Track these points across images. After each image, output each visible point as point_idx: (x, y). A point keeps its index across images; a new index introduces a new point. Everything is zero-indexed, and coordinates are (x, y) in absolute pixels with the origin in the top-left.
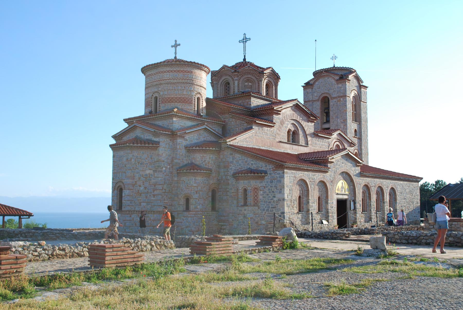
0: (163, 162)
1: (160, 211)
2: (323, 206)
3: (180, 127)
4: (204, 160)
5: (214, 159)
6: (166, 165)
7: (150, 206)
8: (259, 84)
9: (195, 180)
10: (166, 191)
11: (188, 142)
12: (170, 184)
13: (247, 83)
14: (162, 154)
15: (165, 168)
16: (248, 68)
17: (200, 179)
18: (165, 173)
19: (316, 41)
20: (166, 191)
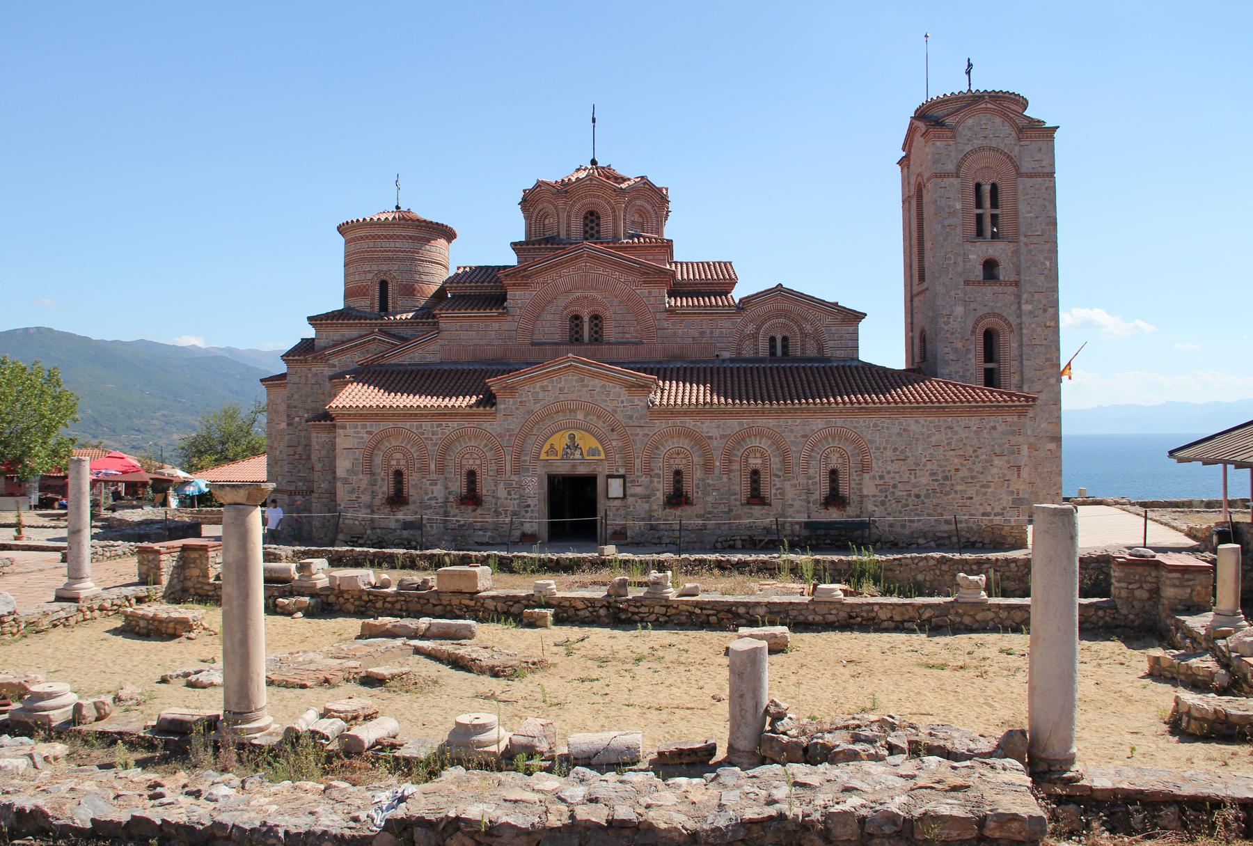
1: (291, 492)
2: (484, 492)
6: (300, 414)
10: (303, 457)
11: (337, 369)
18: (299, 427)
19: (926, 36)
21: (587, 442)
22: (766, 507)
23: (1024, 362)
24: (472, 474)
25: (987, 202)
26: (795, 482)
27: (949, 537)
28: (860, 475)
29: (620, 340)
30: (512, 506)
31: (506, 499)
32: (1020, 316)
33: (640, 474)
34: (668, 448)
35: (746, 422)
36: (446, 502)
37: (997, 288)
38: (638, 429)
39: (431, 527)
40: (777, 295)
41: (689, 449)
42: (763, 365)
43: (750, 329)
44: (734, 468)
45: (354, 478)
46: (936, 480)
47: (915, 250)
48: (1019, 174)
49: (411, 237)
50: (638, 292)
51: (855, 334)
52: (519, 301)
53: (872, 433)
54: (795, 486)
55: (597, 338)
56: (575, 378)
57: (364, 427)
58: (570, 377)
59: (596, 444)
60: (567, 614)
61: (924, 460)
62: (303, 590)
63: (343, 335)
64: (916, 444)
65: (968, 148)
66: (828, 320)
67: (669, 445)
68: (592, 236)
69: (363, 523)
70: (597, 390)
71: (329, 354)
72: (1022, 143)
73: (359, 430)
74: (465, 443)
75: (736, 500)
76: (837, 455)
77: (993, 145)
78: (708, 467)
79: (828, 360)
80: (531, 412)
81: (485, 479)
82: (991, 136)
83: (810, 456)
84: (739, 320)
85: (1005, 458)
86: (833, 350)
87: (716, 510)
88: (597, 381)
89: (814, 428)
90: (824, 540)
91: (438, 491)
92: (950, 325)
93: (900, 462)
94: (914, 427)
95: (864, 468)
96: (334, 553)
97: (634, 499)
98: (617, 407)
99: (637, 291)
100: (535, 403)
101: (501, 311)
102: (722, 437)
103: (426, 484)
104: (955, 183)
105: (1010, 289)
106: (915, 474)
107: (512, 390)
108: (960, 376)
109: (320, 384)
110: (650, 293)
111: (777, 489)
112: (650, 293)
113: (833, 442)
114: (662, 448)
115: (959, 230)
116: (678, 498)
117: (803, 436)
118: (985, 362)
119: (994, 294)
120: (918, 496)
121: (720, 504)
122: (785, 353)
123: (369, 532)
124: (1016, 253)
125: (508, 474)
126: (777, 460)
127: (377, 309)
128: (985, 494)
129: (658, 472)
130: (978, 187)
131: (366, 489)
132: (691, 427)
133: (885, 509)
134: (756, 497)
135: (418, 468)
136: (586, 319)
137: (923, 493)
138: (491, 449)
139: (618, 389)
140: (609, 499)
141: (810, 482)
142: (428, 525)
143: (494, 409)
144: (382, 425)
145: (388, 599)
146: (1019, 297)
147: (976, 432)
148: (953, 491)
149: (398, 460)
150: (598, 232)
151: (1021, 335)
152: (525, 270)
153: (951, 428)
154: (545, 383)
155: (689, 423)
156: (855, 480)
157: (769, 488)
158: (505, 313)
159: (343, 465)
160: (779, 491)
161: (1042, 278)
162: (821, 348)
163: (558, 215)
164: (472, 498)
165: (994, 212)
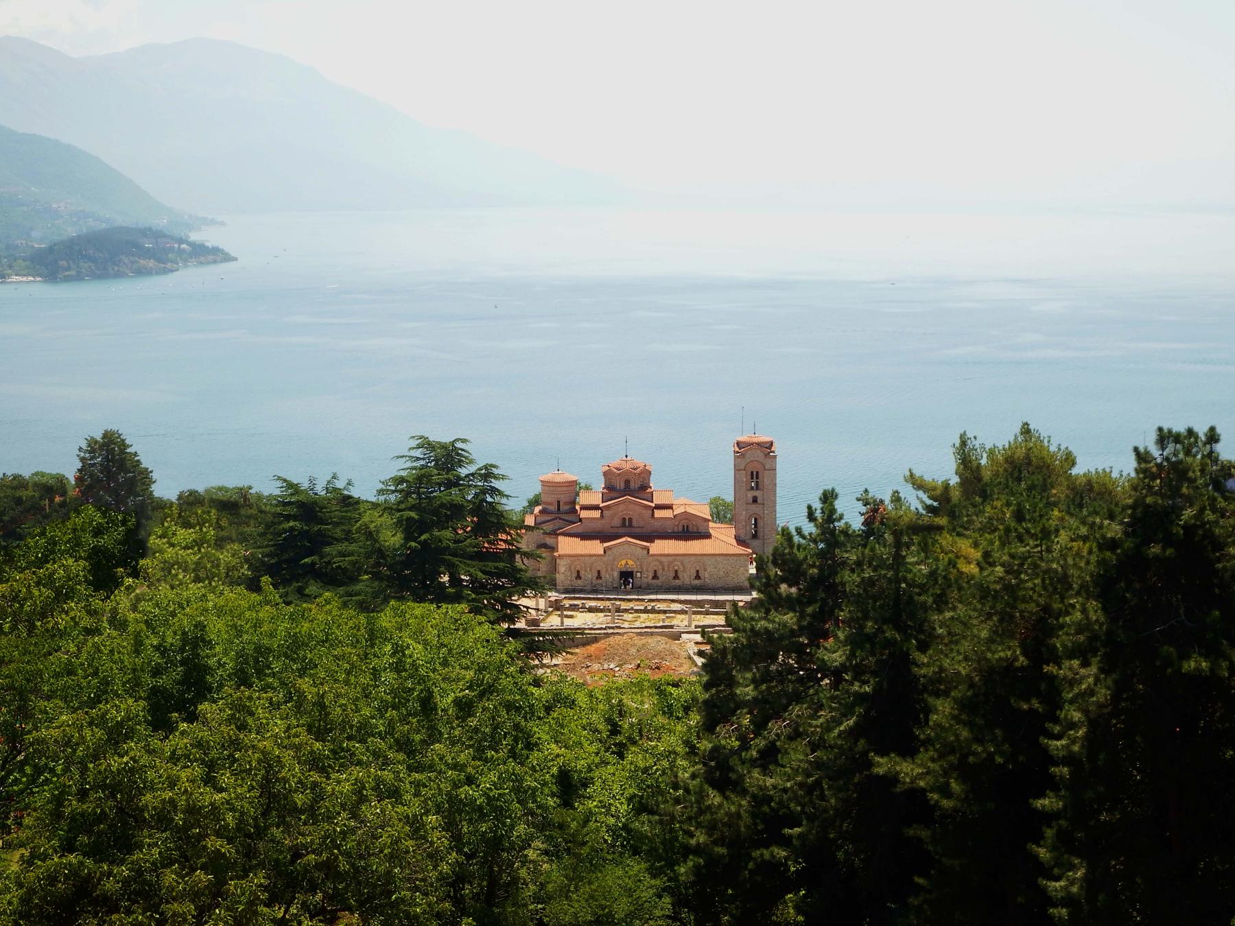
21: (631, 562)
24: (599, 571)
30: (610, 580)
55: (631, 525)
60: (637, 611)
78: (663, 569)
86: (702, 529)
91: (590, 576)
95: (705, 570)
116: (655, 577)
124: (763, 494)
130: (752, 473)
134: (676, 577)
155: (658, 558)
157: (680, 575)
159: (562, 569)
164: (599, 577)
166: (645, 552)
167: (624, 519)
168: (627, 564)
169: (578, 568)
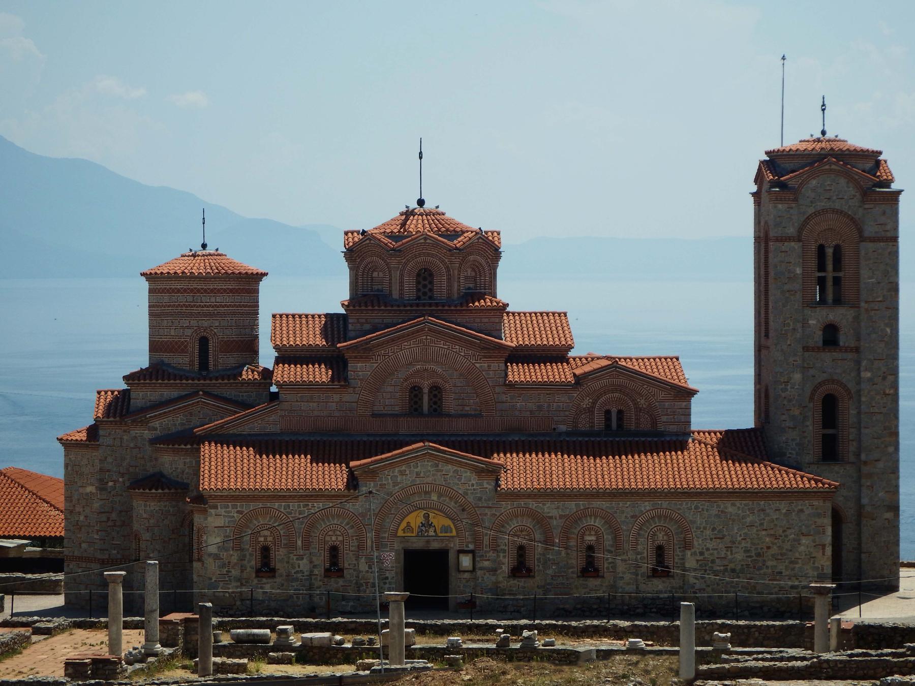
0: (107, 473)
2: (346, 565)
3: (148, 404)
4: (175, 468)
5: (194, 465)
7: (92, 549)
8: (390, 276)
9: (145, 506)
12: (127, 512)
13: (376, 273)
14: (106, 458)
15: (113, 483)
16: (368, 242)
17: (154, 506)
18: (112, 493)
19: (784, 58)
20: (117, 524)
21: (439, 521)
22: (600, 579)
23: (863, 430)
24: (334, 551)
25: (830, 267)
26: (624, 557)
27: (761, 607)
28: (683, 551)
29: (459, 412)
30: (374, 577)
31: (367, 572)
32: (859, 383)
33: (488, 549)
34: (513, 526)
35: (582, 503)
36: (311, 574)
37: (836, 355)
38: (487, 511)
39: (298, 598)
40: (613, 371)
41: (531, 527)
42: (598, 439)
43: (586, 403)
44: (571, 544)
45: (225, 554)
46: (750, 557)
47: (763, 297)
48: (862, 239)
49: (231, 291)
50: (478, 365)
51: (688, 408)
52: (360, 373)
53: (694, 514)
54: (625, 561)
55: (437, 410)
56: (430, 464)
57: (234, 507)
58: (426, 463)
59: (448, 522)
61: (739, 539)
62: (282, 647)
63: (162, 395)
64: (732, 524)
65: (811, 211)
66: (662, 395)
67: (514, 524)
68: (425, 294)
69: (233, 595)
70: (450, 474)
71: (151, 417)
72: (866, 206)
73: (230, 509)
74: (329, 521)
75: (573, 573)
76: (663, 533)
77: (836, 208)
79: (661, 434)
80: (390, 494)
81: (347, 554)
82: (835, 198)
83: (639, 534)
84: (575, 395)
85: (811, 538)
87: (555, 582)
88: (450, 466)
89: (643, 509)
90: (651, 609)
91: (304, 565)
92: (788, 393)
93: (718, 541)
94: (730, 509)
95: (687, 545)
96: (255, 622)
97: (483, 572)
98: (467, 489)
99: (476, 364)
100: (394, 486)
101: (343, 383)
102: (561, 517)
103: (293, 559)
104: (796, 247)
105: (850, 356)
106: (731, 551)
107: (371, 473)
108: (796, 444)
109: (140, 448)
110: (489, 366)
111: (610, 563)
112: (489, 366)
113: (660, 522)
114: (508, 527)
115: (799, 296)
116: (521, 569)
117: (632, 517)
118: (825, 426)
119: (833, 360)
120: (733, 571)
121: (559, 576)
122: (620, 426)
123: (238, 603)
124: (857, 318)
125: (369, 550)
126: (610, 537)
127: (197, 367)
128: (793, 569)
129: (504, 547)
130: (821, 249)
131: (236, 564)
132: (534, 508)
133: (705, 582)
135: (285, 545)
136: (426, 390)
137: (738, 568)
138: (352, 527)
139: (468, 474)
140: (459, 571)
141: (639, 557)
142: (295, 596)
143: (357, 491)
144: (252, 506)
145: (346, 652)
146: (858, 363)
147: (785, 514)
148: (765, 567)
149: (265, 537)
150: (431, 290)
151: (859, 401)
152: (367, 344)
153: (763, 510)
154: (404, 468)
155: (533, 504)
156: (679, 556)
158: (346, 386)
159: (212, 542)
160: (611, 565)
161: (882, 345)
162: (654, 421)
163: (390, 272)
164: (334, 568)
165: (837, 274)
166: (488, 485)
167: (415, 391)
168: (427, 524)
169: (266, 537)
